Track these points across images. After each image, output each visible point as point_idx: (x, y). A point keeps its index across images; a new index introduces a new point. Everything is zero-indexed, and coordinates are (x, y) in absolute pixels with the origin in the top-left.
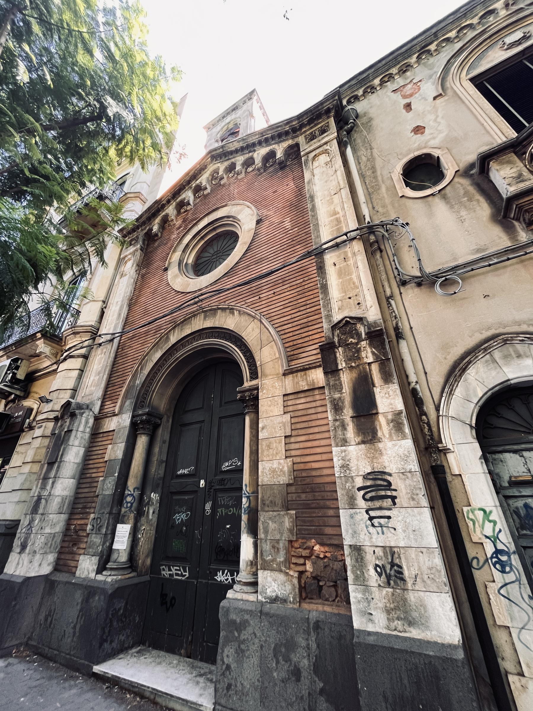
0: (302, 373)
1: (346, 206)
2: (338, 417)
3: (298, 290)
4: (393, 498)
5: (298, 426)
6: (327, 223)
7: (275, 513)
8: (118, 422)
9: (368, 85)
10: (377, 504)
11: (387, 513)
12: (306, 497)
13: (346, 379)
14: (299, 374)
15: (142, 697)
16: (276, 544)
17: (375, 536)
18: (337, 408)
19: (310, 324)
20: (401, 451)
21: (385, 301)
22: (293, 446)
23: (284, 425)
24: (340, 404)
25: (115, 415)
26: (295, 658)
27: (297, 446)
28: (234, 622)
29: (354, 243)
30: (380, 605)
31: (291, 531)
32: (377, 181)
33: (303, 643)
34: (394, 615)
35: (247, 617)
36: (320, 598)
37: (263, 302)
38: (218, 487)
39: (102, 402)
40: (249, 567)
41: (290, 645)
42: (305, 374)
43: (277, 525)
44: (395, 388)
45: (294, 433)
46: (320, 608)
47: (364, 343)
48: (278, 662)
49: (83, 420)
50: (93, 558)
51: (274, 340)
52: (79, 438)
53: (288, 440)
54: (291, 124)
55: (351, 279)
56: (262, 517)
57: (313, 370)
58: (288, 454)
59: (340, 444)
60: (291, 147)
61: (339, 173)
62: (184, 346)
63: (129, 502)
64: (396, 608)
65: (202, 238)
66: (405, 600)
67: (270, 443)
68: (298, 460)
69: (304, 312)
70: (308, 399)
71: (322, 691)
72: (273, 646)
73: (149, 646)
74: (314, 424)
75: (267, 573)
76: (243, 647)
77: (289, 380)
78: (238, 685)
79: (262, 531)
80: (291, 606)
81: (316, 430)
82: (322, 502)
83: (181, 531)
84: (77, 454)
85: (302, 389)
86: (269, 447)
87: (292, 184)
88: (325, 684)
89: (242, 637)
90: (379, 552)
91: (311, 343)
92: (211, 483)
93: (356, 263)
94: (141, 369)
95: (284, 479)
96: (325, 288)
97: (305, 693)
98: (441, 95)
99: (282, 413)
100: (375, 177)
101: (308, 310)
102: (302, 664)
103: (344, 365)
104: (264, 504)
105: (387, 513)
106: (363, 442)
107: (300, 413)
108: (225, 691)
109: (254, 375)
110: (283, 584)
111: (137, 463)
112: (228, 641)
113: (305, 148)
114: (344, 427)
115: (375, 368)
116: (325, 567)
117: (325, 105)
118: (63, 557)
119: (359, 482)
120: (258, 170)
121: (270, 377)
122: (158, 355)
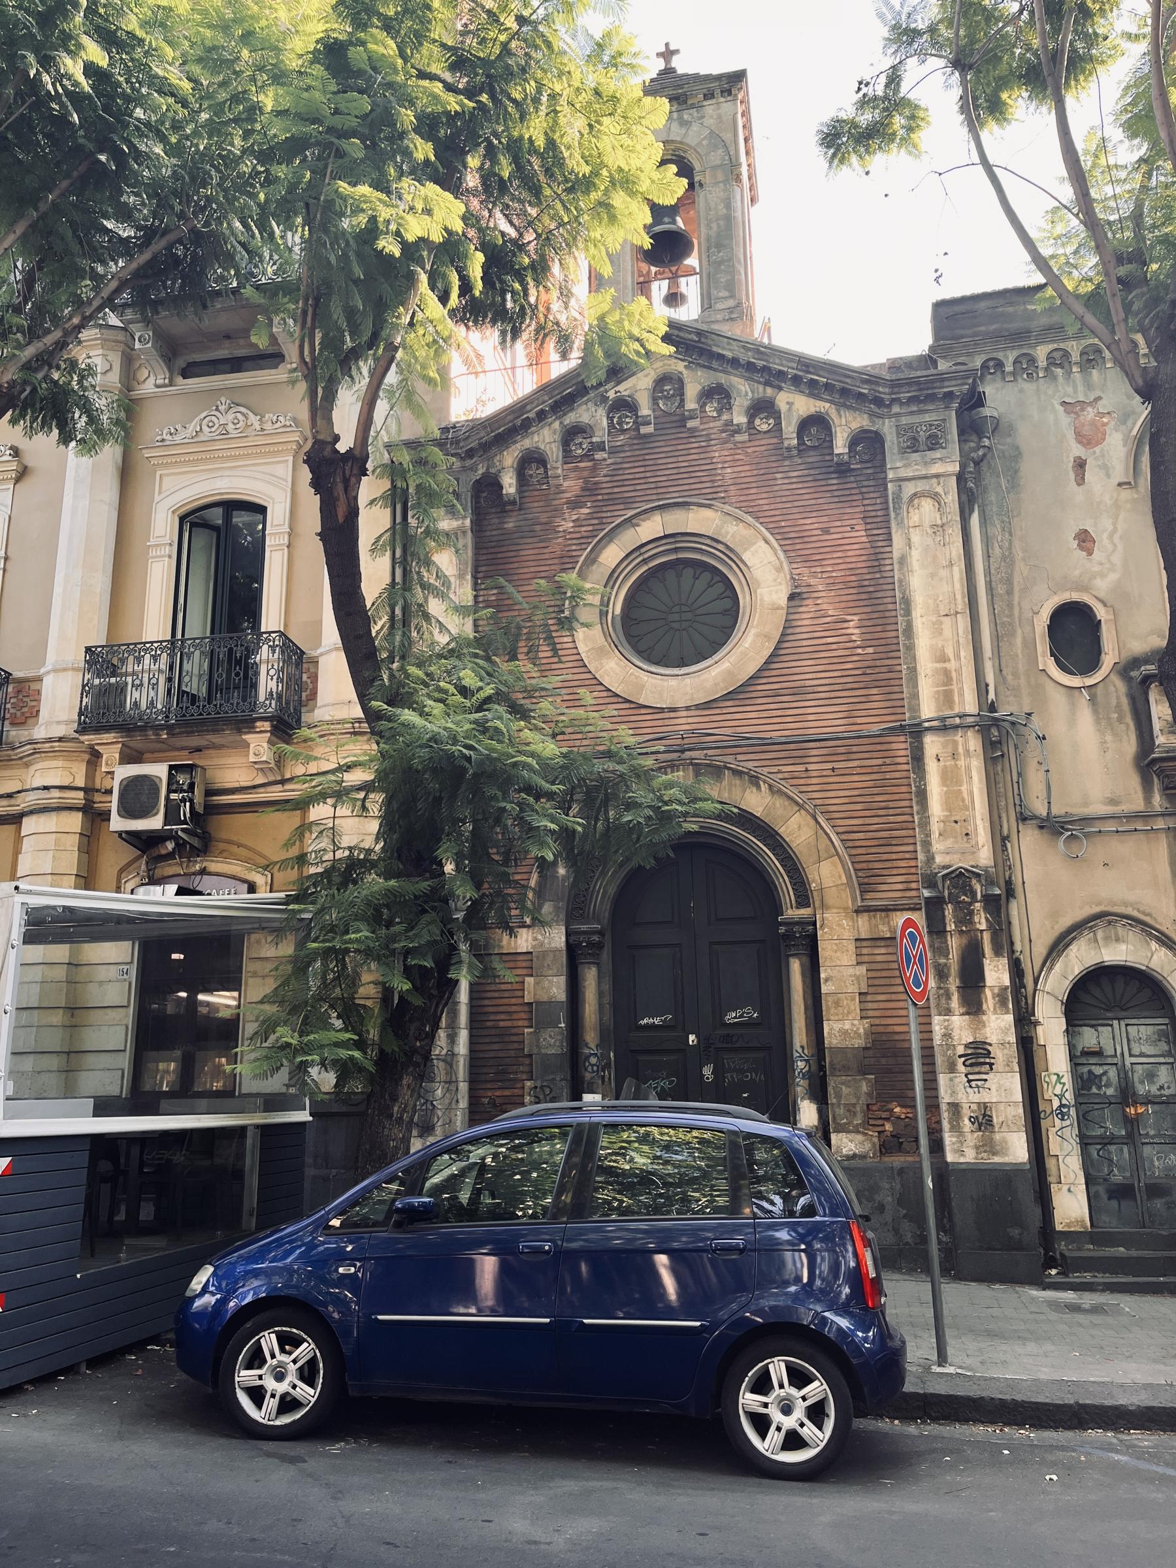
0: (883, 914)
1: (963, 654)
5: (877, 982)
6: (929, 672)
8: (535, 939)
9: (1025, 351)
10: (977, 1069)
11: (984, 1077)
13: (954, 944)
14: (878, 914)
18: (942, 974)
20: (1003, 1024)
21: (1001, 841)
22: (870, 1005)
23: (858, 978)
27: (875, 1005)
29: (970, 733)
31: (869, 1095)
32: (1011, 616)
37: (814, 781)
38: (721, 1045)
42: (887, 916)
43: (849, 1091)
44: (1004, 962)
45: (872, 990)
47: (978, 905)
51: (838, 854)
55: (960, 792)
56: (832, 1083)
61: (956, 569)
65: (645, 561)
67: (839, 999)
68: (877, 1021)
71: (905, 1216)
75: (842, 1135)
77: (863, 922)
85: (882, 935)
86: (837, 1004)
87: (860, 534)
90: (974, 1107)
91: (895, 872)
93: (968, 769)
95: (859, 1043)
96: (922, 795)
97: (889, 1220)
98: (1129, 483)
100: (1010, 606)
101: (892, 819)
105: (984, 1077)
106: (967, 1013)
107: (879, 966)
109: (804, 898)
110: (862, 1143)
111: (592, 1009)
115: (986, 937)
116: (906, 1126)
117: (946, 384)
119: (961, 1050)
120: (789, 449)
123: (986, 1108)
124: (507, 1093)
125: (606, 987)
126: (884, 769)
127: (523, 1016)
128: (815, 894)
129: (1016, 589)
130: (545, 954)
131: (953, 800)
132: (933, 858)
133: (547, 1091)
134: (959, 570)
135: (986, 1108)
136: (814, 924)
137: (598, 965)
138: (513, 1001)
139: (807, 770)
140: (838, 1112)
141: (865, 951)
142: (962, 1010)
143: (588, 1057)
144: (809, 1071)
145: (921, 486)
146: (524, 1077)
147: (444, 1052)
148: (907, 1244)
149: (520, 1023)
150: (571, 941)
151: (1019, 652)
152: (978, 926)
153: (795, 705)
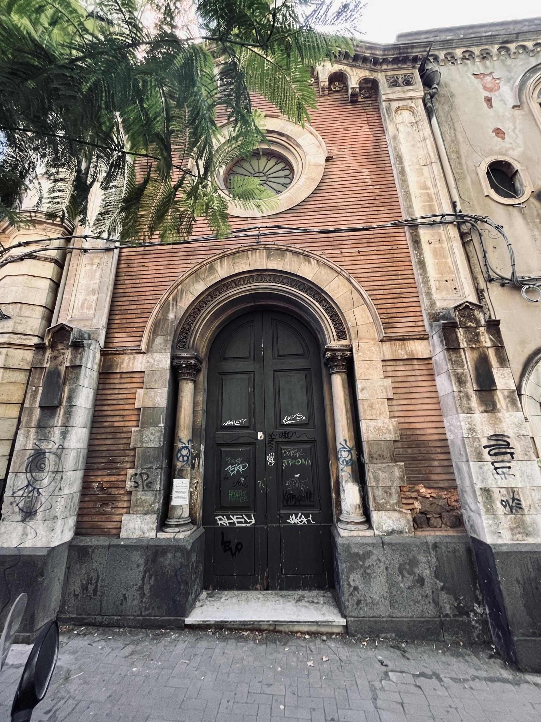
0: (401, 342)
1: (438, 184)
2: (462, 389)
3: (386, 256)
4: (512, 454)
5: (399, 391)
6: (418, 195)
7: (384, 465)
10: (500, 458)
12: (412, 451)
14: (397, 343)
15: (261, 631)
16: (388, 490)
17: (500, 481)
19: (403, 296)
21: (479, 293)
24: (463, 378)
25: (140, 352)
26: (417, 571)
27: (400, 408)
28: (357, 554)
29: (450, 227)
30: (506, 526)
32: (462, 169)
33: (424, 560)
34: (516, 531)
35: (369, 549)
36: (429, 526)
38: (280, 440)
39: (107, 333)
40: (358, 510)
41: (414, 563)
42: (404, 344)
46: (432, 533)
47: (482, 329)
48: (403, 576)
49: (91, 352)
50: (147, 517)
52: (88, 377)
53: (390, 403)
54: (373, 51)
55: (446, 263)
57: (411, 342)
58: (392, 414)
59: (466, 411)
60: (366, 80)
61: (428, 142)
62: (237, 283)
63: (186, 456)
64: (518, 527)
66: (523, 521)
67: (372, 404)
68: (402, 420)
69: (396, 282)
70: (408, 368)
71: (442, 589)
72: (397, 566)
73: (214, 589)
74: (414, 390)
76: (368, 571)
77: (387, 346)
78: (368, 599)
79: (372, 480)
80: (407, 535)
81: (418, 396)
82: (427, 456)
83: (239, 482)
84: (87, 397)
85: (401, 357)
86: (371, 407)
88: (445, 582)
89: (367, 564)
90: (504, 491)
92: (271, 435)
94: (175, 299)
95: (391, 437)
98: (519, 106)
99: (382, 377)
100: (460, 164)
101: (400, 281)
102: (424, 574)
103: (465, 345)
104: (372, 458)
105: (508, 465)
106: (486, 411)
107: (400, 379)
108: (355, 606)
109: (342, 334)
111: (187, 413)
112: (351, 570)
113: (385, 91)
114: (468, 397)
116: (431, 504)
117: (415, 50)
118: (86, 519)
119: (485, 442)
121: (365, 341)
122: (200, 287)
123: (514, 492)
124: (113, 478)
125: (200, 399)
126: (392, 252)
127: (134, 418)
128: (351, 329)
129: (463, 156)
130: (153, 373)
131: (441, 268)
132: (435, 303)
133: (145, 477)
134: (430, 142)
135: (514, 492)
136: (351, 350)
137: (195, 382)
138: (127, 407)
139: (341, 252)
140: (376, 493)
141: (389, 369)
142: (482, 409)
143: (180, 450)
144: (351, 459)
145: (402, 103)
146: (128, 465)
147: (56, 446)
148: (447, 615)
149: (130, 424)
150: (174, 363)
151: (470, 187)
152: (484, 344)
153: (332, 216)
